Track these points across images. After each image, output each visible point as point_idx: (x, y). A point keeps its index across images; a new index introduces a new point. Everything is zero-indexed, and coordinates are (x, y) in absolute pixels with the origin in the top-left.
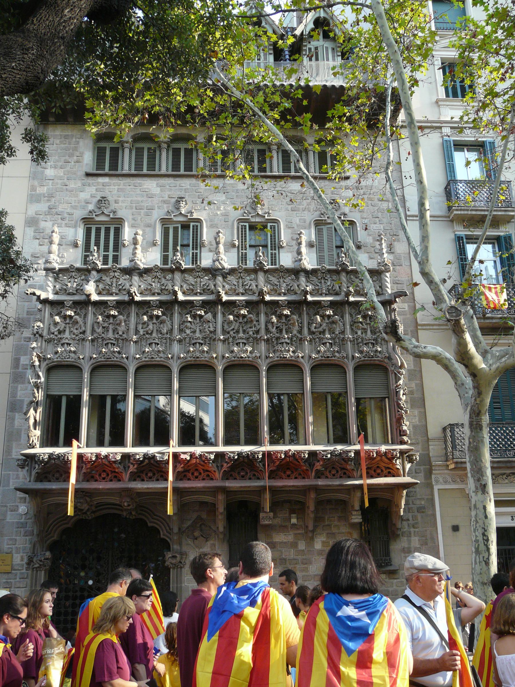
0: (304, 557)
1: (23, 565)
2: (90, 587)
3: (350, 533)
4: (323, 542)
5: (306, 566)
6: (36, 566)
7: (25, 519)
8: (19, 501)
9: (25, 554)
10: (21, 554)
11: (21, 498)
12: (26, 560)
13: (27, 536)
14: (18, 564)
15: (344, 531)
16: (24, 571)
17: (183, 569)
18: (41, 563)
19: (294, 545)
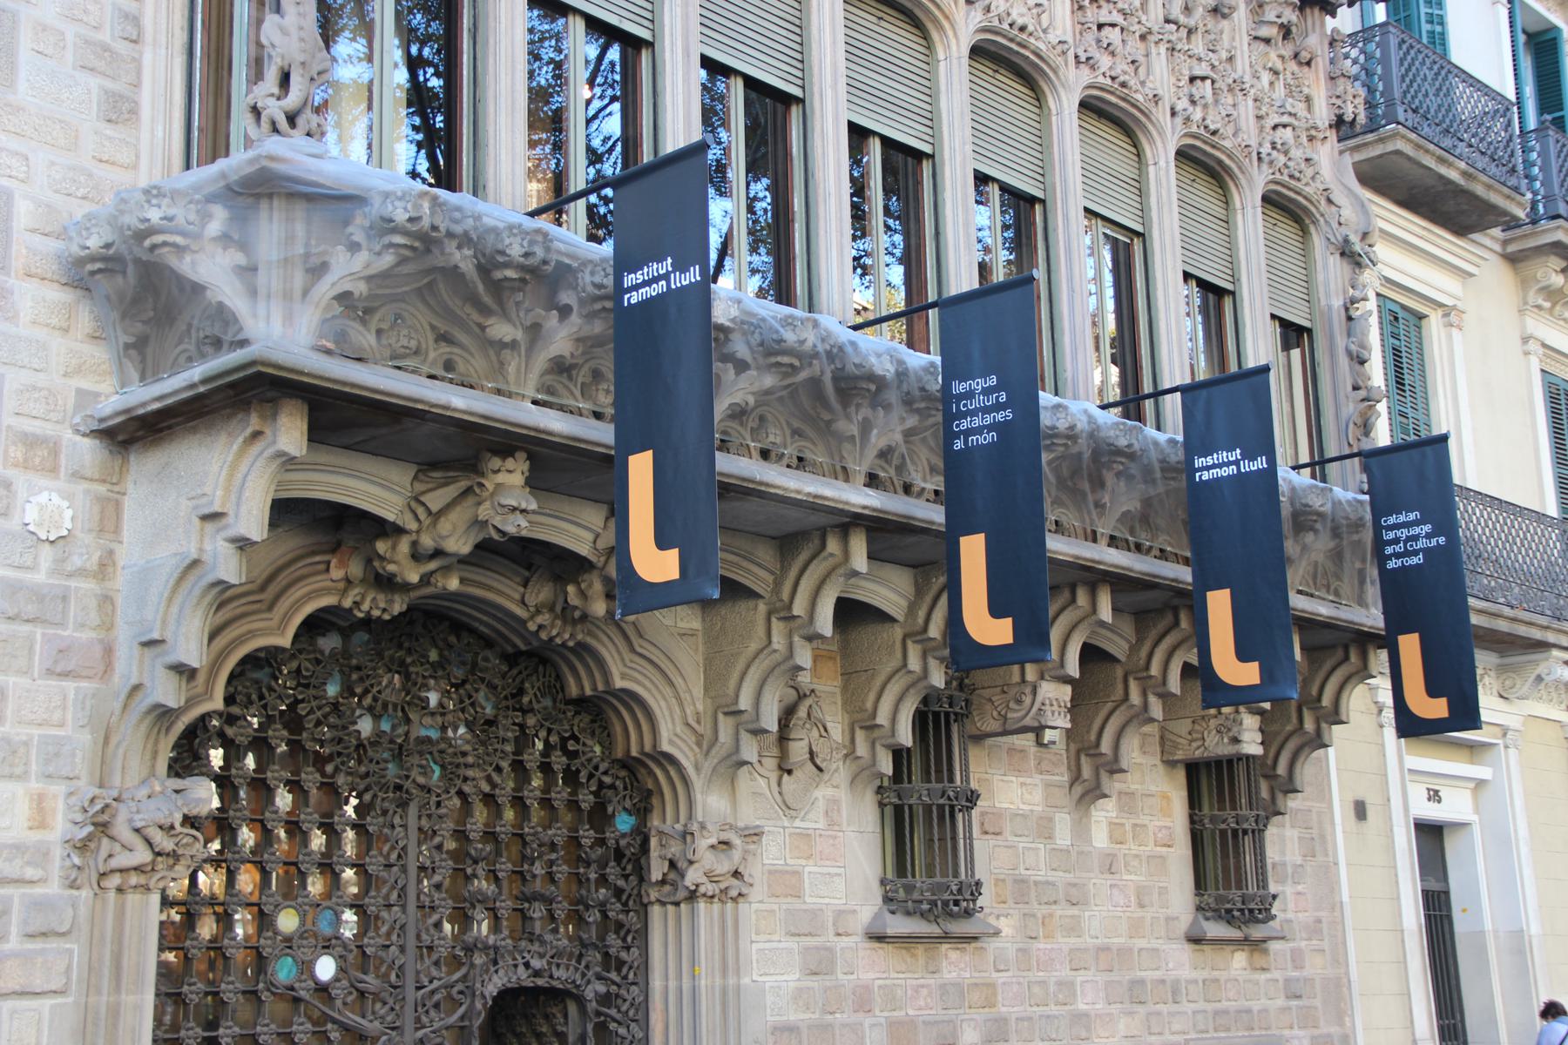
0: (1069, 877)
1: (43, 854)
2: (323, 989)
3: (1166, 797)
4: (1113, 826)
5: (1074, 911)
6: (123, 860)
7: (54, 572)
8: (17, 452)
9: (59, 789)
10: (35, 785)
11: (31, 442)
12: (62, 825)
13: (65, 675)
14: (18, 848)
15: (1153, 788)
16: (54, 888)
17: (742, 906)
18: (167, 844)
19: (1045, 830)
